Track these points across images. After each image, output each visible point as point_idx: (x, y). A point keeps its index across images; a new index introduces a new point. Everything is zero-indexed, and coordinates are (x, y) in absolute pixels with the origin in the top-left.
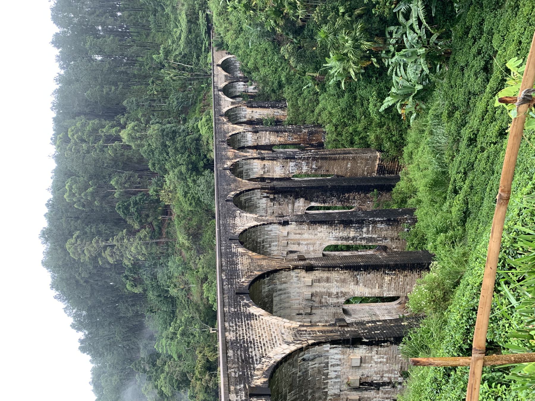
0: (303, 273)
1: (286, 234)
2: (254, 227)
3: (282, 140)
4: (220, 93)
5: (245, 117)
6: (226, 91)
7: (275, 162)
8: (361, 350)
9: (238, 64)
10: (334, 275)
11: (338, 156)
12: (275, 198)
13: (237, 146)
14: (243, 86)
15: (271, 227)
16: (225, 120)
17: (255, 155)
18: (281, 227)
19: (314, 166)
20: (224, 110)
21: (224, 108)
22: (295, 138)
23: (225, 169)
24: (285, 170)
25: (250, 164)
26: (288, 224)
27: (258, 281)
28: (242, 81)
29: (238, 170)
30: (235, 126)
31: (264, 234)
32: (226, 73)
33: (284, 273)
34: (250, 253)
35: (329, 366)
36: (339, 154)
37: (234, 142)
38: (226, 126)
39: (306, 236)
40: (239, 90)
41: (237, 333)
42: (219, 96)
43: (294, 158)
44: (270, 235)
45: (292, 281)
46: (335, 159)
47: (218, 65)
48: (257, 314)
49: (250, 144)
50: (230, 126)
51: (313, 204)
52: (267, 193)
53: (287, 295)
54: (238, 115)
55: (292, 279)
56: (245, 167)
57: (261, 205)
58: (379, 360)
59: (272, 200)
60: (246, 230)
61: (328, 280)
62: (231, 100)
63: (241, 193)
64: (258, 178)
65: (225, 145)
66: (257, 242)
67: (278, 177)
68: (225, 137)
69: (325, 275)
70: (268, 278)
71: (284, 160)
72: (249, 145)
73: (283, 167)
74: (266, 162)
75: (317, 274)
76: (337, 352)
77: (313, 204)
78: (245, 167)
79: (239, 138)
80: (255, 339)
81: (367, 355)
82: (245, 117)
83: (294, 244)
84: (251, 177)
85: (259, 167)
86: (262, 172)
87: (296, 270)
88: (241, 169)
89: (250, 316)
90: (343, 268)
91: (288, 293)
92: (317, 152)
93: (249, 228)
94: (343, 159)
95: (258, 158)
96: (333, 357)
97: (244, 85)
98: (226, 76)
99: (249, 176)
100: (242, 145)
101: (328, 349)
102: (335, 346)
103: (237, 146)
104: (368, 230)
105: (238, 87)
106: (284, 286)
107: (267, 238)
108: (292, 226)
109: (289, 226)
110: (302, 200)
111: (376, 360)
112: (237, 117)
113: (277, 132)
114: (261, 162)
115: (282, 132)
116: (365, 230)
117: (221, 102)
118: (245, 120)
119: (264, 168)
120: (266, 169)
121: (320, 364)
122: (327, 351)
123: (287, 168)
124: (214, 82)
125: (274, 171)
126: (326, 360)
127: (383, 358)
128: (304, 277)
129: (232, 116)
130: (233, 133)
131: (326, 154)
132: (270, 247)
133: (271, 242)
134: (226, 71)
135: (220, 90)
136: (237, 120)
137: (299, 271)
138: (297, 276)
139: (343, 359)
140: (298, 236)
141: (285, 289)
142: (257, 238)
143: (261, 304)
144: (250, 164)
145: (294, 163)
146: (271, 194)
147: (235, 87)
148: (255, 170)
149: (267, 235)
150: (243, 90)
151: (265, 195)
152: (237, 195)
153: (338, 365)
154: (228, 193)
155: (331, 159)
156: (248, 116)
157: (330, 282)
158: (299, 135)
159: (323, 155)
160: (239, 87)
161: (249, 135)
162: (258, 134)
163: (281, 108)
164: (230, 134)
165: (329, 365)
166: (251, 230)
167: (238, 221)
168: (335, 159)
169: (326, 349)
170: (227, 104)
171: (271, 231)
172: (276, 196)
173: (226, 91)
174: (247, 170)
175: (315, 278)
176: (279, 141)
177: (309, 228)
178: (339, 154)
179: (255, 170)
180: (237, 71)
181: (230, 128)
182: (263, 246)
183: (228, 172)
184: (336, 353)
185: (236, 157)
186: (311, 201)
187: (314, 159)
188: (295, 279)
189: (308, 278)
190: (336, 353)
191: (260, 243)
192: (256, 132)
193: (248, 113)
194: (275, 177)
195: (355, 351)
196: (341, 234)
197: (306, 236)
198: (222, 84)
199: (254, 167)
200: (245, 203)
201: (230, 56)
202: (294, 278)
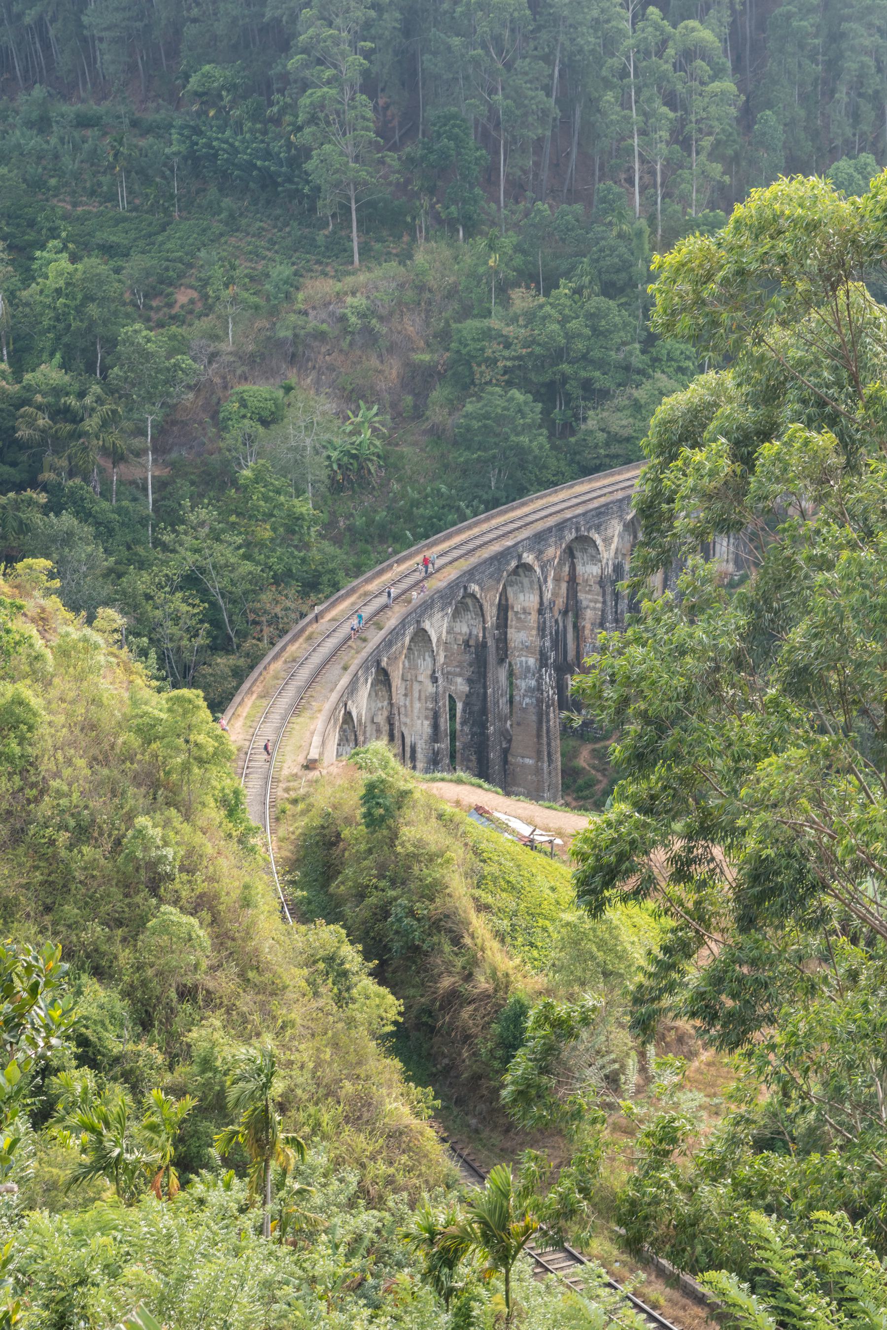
0: (386, 714)
7: (534, 632)
11: (545, 740)
13: (575, 545)
15: (429, 660)
16: (629, 517)
17: (548, 596)
18: (429, 672)
23: (520, 557)
25: (532, 588)
36: (549, 744)
39: (417, 705)
46: (539, 736)
49: (580, 569)
51: (459, 706)
56: (526, 581)
57: (458, 624)
59: (467, 643)
65: (570, 536)
68: (589, 530)
77: (459, 706)
78: (526, 581)
85: (526, 604)
86: (517, 608)
94: (539, 753)
95: (541, 603)
100: (578, 554)
103: (575, 545)
108: (430, 689)
110: (466, 689)
125: (519, 630)
130: (599, 542)
131: (548, 721)
140: (416, 695)
144: (532, 588)
148: (521, 596)
152: (473, 596)
155: (539, 729)
159: (548, 714)
161: (593, 570)
168: (539, 736)
172: (473, 649)
178: (549, 744)
179: (521, 596)
181: (610, 532)
183: (514, 564)
187: (540, 701)
192: (601, 582)
194: (509, 631)
196: (419, 750)
197: (417, 705)
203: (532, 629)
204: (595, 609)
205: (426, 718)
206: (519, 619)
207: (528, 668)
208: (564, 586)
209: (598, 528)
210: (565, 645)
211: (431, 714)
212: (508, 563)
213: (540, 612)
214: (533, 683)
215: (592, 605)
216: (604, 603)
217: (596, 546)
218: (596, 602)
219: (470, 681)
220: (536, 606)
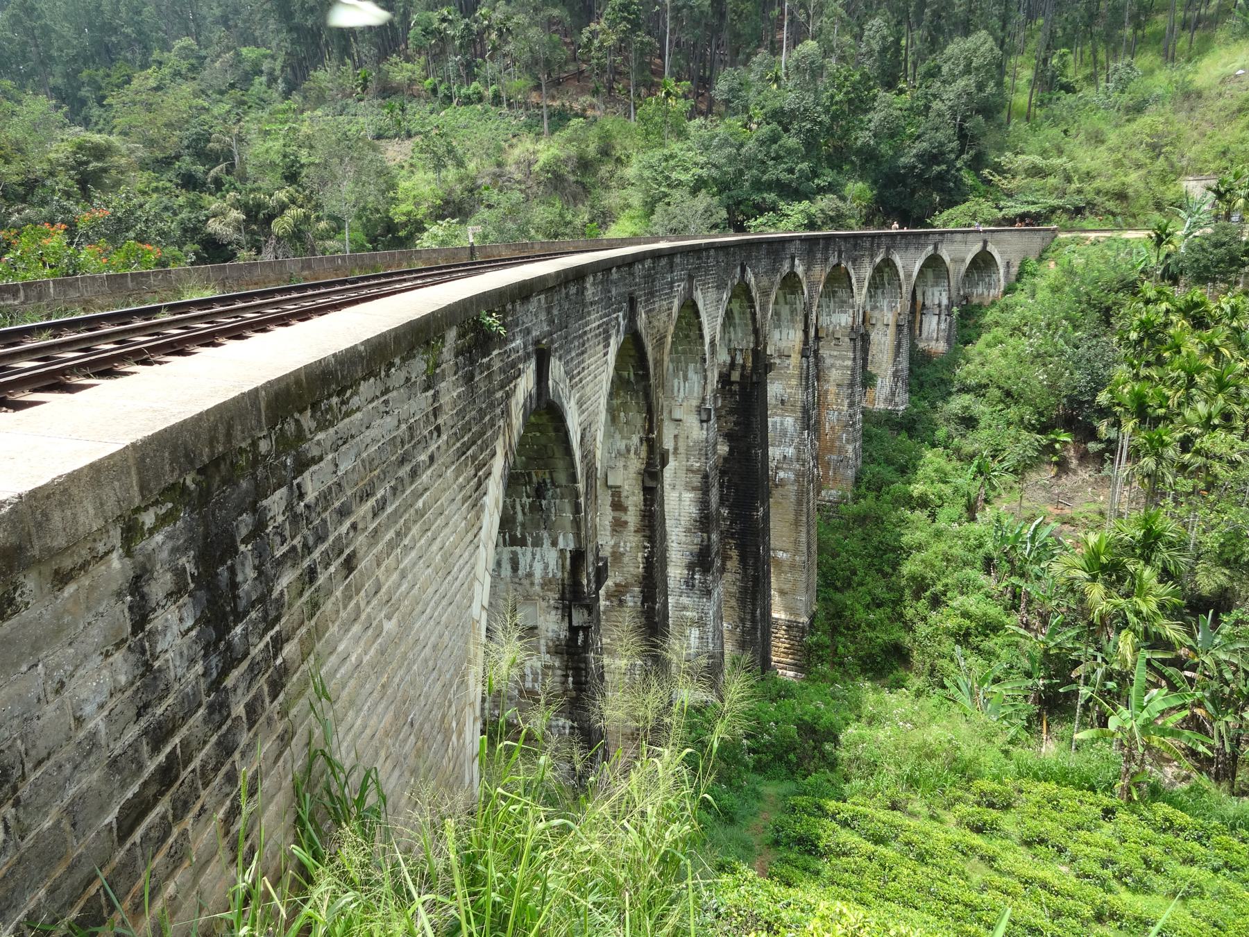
0: (636, 464)
1: (677, 415)
3: (831, 397)
4: (931, 248)
6: (934, 264)
7: (794, 382)
8: (555, 627)
9: (980, 291)
10: (631, 542)
12: (732, 383)
15: (694, 377)
16: (878, 260)
18: (695, 403)
19: (781, 474)
20: (898, 259)
24: (775, 406)
26: (702, 421)
27: (632, 353)
30: (866, 284)
31: (679, 361)
32: (968, 261)
33: (638, 419)
34: (672, 329)
35: (514, 548)
37: (838, 281)
38: (867, 260)
40: (929, 293)
41: (591, 304)
42: (925, 245)
44: (675, 375)
45: (618, 436)
47: (985, 243)
48: (609, 356)
49: (824, 320)
50: (867, 272)
52: (743, 367)
54: (879, 291)
55: (623, 438)
58: (528, 671)
59: (725, 379)
60: (698, 316)
61: (618, 526)
62: (915, 274)
63: (751, 300)
65: (833, 260)
69: (632, 518)
70: (632, 378)
72: (820, 319)
73: (783, 402)
74: (795, 359)
75: (634, 500)
76: (550, 569)
78: (785, 311)
79: (839, 294)
80: (586, 355)
81: (543, 642)
82: (874, 308)
85: (783, 344)
87: (644, 448)
90: (649, 562)
93: (700, 323)
94: (796, 542)
95: (806, 342)
96: (538, 557)
97: (939, 305)
98: (963, 261)
101: (561, 545)
102: (568, 561)
104: (685, 608)
105: (936, 291)
109: (696, 424)
111: (528, 664)
112: (877, 288)
113: (852, 385)
114: (797, 348)
115: (852, 395)
116: (685, 600)
117: (913, 251)
119: (780, 356)
120: (778, 361)
121: (523, 525)
122: (554, 543)
124: (952, 232)
126: (529, 540)
127: (535, 680)
128: (625, 467)
129: (884, 275)
130: (854, 281)
131: (808, 502)
134: (974, 261)
135: (936, 248)
137: (644, 454)
138: (628, 451)
139: (532, 584)
144: (793, 321)
145: (790, 429)
146: (742, 375)
147: (936, 284)
148: (776, 335)
149: (676, 370)
151: (739, 360)
153: (515, 568)
155: (798, 513)
156: (876, 314)
157: (614, 530)
160: (937, 294)
161: (843, 319)
162: (847, 339)
163: (893, 394)
164: (852, 272)
165: (518, 549)
166: (695, 329)
167: (712, 294)
169: (561, 539)
170: (909, 263)
172: (735, 388)
173: (934, 264)
175: (624, 494)
176: (827, 391)
177: (692, 471)
178: (808, 532)
179: (776, 335)
183: (786, 268)
184: (546, 566)
185: (812, 285)
186: (723, 473)
188: (621, 445)
189: (626, 478)
190: (546, 566)
193: (888, 314)
195: (553, 612)
198: (945, 254)
199: (785, 332)
201: (1002, 271)
202: (624, 442)
203: (791, 377)
207: (784, 433)
209: (854, 261)
211: (696, 480)
212: (782, 259)
213: (804, 354)
214: (790, 451)
215: (838, 363)
218: (843, 358)
219: (730, 437)
220: (798, 345)
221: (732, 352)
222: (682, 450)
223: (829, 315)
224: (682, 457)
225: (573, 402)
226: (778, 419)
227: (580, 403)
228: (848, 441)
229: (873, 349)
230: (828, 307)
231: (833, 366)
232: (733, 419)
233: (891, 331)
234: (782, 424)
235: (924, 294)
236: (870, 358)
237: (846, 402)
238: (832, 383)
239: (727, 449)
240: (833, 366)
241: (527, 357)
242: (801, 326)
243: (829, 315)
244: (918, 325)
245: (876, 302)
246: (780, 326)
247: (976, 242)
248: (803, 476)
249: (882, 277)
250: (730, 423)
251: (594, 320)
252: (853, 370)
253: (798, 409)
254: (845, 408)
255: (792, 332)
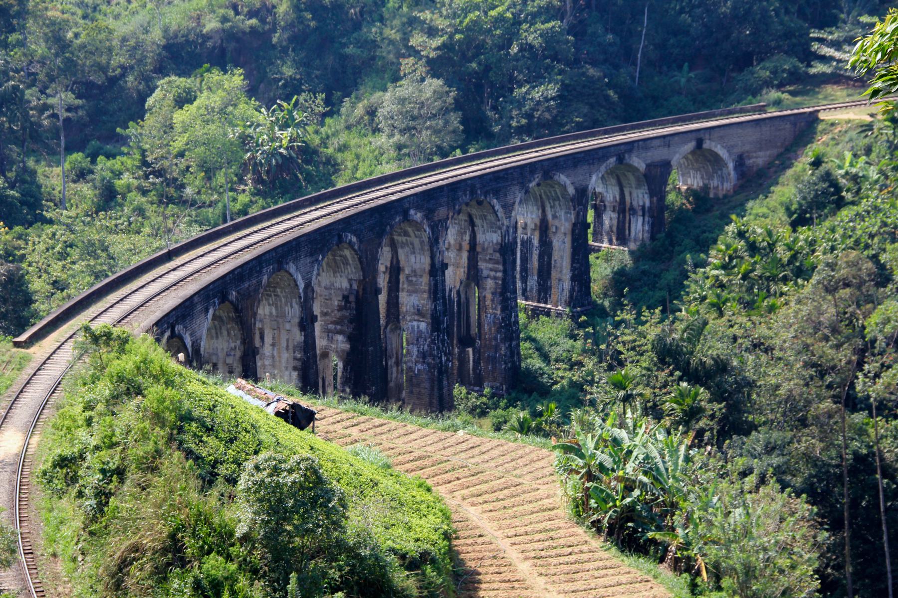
2: (297, 285)
3: (488, 302)
5: (555, 217)
7: (425, 295)
14: (641, 203)
21: (568, 176)
22: (490, 329)
28: (651, 202)
29: (410, 230)
40: (634, 195)
43: (433, 331)
44: (286, 305)
49: (480, 238)
52: (358, 292)
53: (214, 335)
64: (398, 261)
66: (275, 287)
67: (401, 300)
71: (429, 312)
83: (273, 338)
84: (400, 251)
85: (417, 266)
88: (412, 234)
89: (207, 311)
91: (217, 337)
92: (446, 371)
95: (433, 265)
99: (402, 247)
100: (478, 222)
106: (225, 333)
107: (281, 301)
110: (346, 346)
118: (550, 217)
120: (414, 279)
123: (416, 317)
130: (497, 208)
132: (269, 305)
133: (276, 307)
136: (548, 199)
140: (284, 345)
141: (221, 333)
142: (282, 288)
143: (196, 299)
150: (635, 204)
154: (354, 233)
155: (431, 396)
158: (496, 339)
160: (640, 196)
171: (292, 307)
172: (353, 305)
174: (412, 244)
176: (485, 297)
180: (702, 178)
181: (510, 198)
182: (270, 296)
188: (233, 345)
191: (274, 291)
199: (418, 257)
200: (340, 256)
201: (731, 165)
204: (495, 278)
205: (295, 368)
206: (410, 282)
208: (465, 255)
209: (497, 193)
210: (468, 317)
211: (299, 364)
215: (492, 274)
216: (505, 272)
217: (495, 213)
219: (350, 339)
220: (427, 268)
221: (350, 281)
222: (291, 347)
223: (484, 233)
224: (291, 351)
225: (187, 335)
226: (415, 323)
227: (191, 335)
228: (501, 340)
229: (556, 256)
230: (483, 226)
231: (488, 277)
232: (352, 326)
233: (568, 239)
234: (418, 327)
235: (631, 194)
236: (553, 262)
237: (499, 307)
238: (488, 291)
239: (349, 346)
240: (488, 277)
241: (168, 328)
242: (428, 254)
243: (484, 233)
244: (627, 225)
245: (555, 212)
246: (414, 253)
247: (685, 143)
248: (434, 368)
249: (555, 191)
250: (348, 330)
251: (199, 308)
252: (504, 280)
253: (429, 316)
254: (499, 312)
255: (423, 257)
